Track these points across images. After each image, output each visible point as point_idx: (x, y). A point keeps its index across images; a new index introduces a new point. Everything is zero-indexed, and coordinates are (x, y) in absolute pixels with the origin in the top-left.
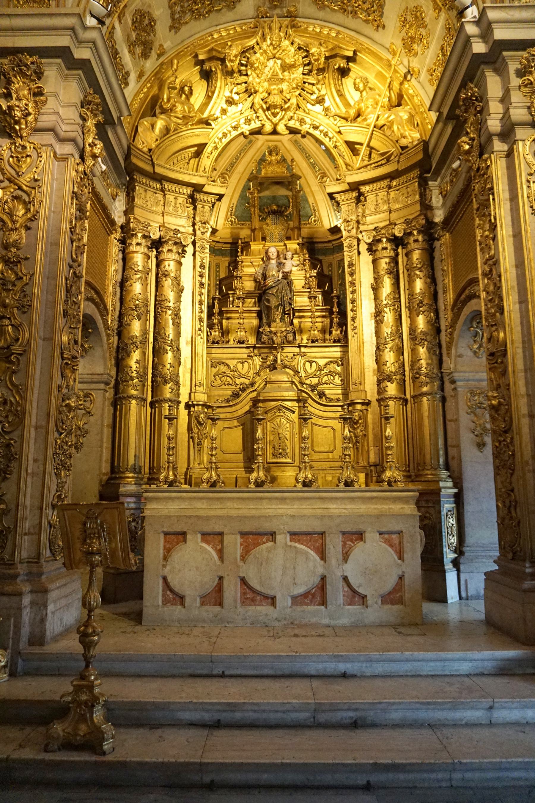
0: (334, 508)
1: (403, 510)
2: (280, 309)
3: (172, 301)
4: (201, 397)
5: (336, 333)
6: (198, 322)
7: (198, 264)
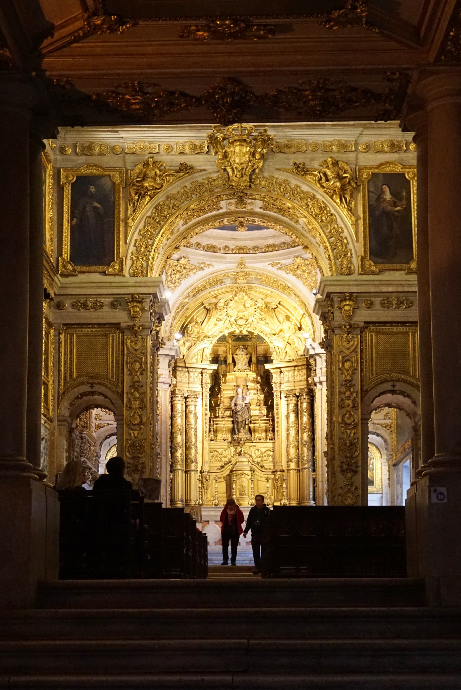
2: (244, 422)
3: (194, 425)
4: (206, 469)
6: (205, 432)
7: (204, 404)
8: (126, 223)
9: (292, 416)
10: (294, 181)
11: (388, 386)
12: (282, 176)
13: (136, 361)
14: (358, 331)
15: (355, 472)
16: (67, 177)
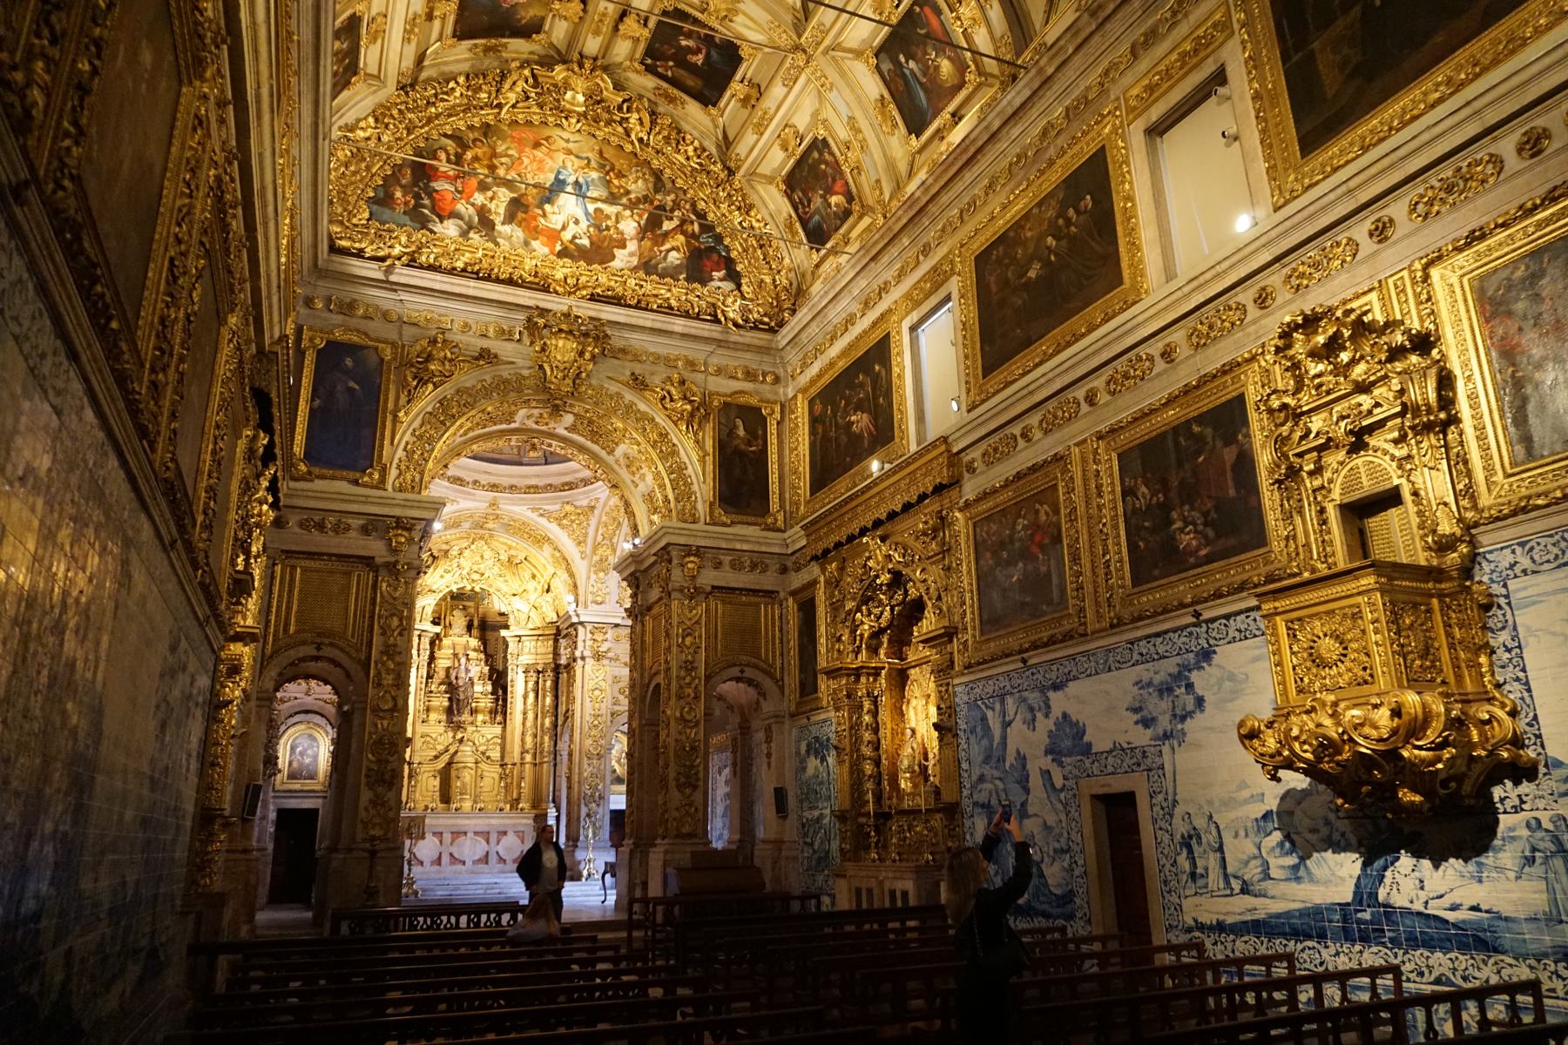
0: (493, 821)
1: (526, 822)
5: (499, 718)
8: (395, 417)
9: (531, 696)
10: (629, 396)
11: (735, 672)
12: (613, 388)
13: (393, 615)
14: (702, 597)
15: (695, 787)
16: (311, 339)
